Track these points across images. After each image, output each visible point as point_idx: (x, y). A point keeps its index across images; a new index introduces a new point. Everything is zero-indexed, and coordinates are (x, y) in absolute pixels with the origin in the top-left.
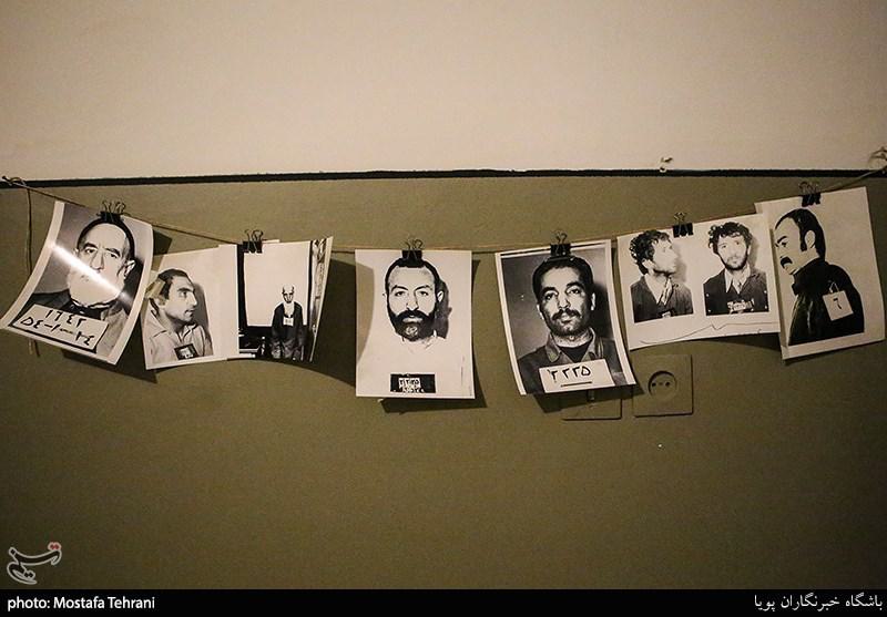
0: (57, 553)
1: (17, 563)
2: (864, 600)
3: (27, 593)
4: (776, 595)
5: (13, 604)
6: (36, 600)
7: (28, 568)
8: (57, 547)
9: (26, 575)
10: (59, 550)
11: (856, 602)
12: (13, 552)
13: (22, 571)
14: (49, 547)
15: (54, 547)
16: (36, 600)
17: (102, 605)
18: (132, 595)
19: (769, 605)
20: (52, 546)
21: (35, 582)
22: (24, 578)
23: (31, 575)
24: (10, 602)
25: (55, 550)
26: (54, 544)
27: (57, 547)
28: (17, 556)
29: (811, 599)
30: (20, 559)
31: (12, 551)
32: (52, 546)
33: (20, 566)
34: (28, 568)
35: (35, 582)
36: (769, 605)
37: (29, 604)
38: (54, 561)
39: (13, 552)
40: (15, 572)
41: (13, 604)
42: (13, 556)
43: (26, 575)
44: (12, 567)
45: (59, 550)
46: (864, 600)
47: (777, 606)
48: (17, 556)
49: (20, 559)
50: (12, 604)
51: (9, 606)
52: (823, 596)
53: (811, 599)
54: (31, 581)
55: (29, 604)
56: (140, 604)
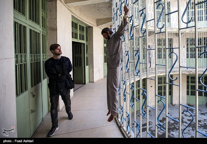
0: (13, 129)
1: (6, 132)
5: (5, 141)
7: (7, 133)
9: (6, 134)
12: (3, 129)
13: (5, 133)
14: (12, 128)
18: (29, 139)
20: (12, 128)
22: (5, 134)
23: (8, 134)
25: (13, 128)
27: (14, 128)
28: (4, 130)
30: (5, 130)
32: (12, 128)
34: (7, 133)
37: (8, 141)
39: (3, 129)
40: (4, 133)
41: (5, 141)
43: (6, 134)
44: (3, 132)
45: (14, 128)
48: (4, 130)
50: (4, 141)
51: (4, 142)
54: (7, 136)
55: (8, 141)
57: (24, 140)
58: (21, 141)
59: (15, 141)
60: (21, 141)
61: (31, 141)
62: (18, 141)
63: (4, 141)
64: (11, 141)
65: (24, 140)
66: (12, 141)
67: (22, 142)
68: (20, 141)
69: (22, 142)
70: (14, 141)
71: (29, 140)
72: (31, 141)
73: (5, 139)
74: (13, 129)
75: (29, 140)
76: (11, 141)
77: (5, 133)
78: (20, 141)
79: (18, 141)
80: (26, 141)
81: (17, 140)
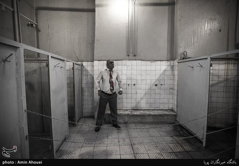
0: (16, 149)
1: (5, 152)
2: (232, 162)
3: (8, 160)
4: (209, 161)
5: (3, 163)
6: (11, 162)
7: (8, 153)
8: (16, 147)
9: (7, 155)
10: (16, 148)
11: (230, 162)
12: (4, 148)
13: (6, 154)
14: (13, 147)
15: (15, 147)
16: (11, 162)
17: (30, 162)
19: (207, 163)
20: (14, 147)
21: (10, 157)
22: (7, 155)
23: (9, 155)
24: (3, 162)
25: (15, 148)
26: (15, 146)
27: (16, 147)
28: (5, 150)
29: (218, 161)
30: (6, 150)
31: (4, 148)
32: (14, 147)
33: (6, 152)
34: (8, 153)
35: (10, 157)
36: (207, 163)
38: (15, 151)
39: (4, 148)
40: (4, 154)
41: (3, 163)
42: (4, 150)
44: (4, 153)
46: (232, 162)
47: (210, 163)
48: (5, 150)
49: (6, 150)
50: (4, 163)
51: (3, 163)
52: (221, 161)
53: (218, 161)
54: (9, 156)
56: (40, 162)
63: (4, 163)
64: (13, 163)
66: (15, 163)
74: (16, 149)
76: (13, 163)
77: (6, 154)
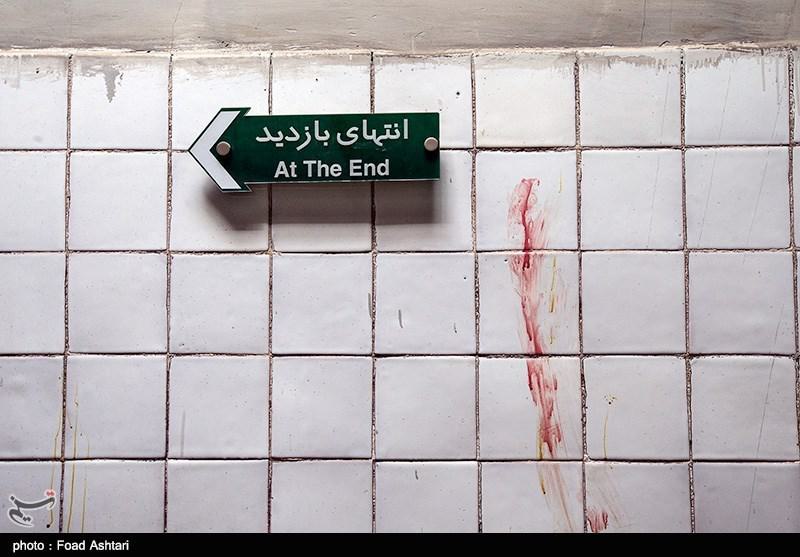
0: (52, 500)
1: (21, 509)
5: (17, 546)
7: (27, 513)
9: (25, 519)
12: (12, 498)
13: (21, 515)
20: (48, 494)
21: (33, 526)
22: (23, 522)
23: (29, 519)
27: (52, 494)
28: (17, 502)
32: (48, 494)
35: (33, 526)
37: (30, 546)
39: (12, 498)
40: (14, 516)
43: (25, 519)
44: (12, 512)
48: (17, 502)
50: (16, 546)
51: (15, 549)
54: (29, 527)
55: (30, 546)
57: (94, 542)
58: (82, 546)
59: (59, 545)
60: (82, 546)
61: (120, 546)
62: (68, 546)
63: (16, 546)
64: (41, 546)
65: (94, 542)
66: (47, 547)
67: (84, 548)
68: (76, 546)
69: (84, 548)
70: (55, 545)
71: (113, 543)
72: (120, 546)
73: (18, 537)
74: (52, 500)
75: (113, 543)
76: (41, 546)
77: (21, 515)
78: (76, 546)
79: (68, 546)
80: (101, 544)
81: (64, 543)
